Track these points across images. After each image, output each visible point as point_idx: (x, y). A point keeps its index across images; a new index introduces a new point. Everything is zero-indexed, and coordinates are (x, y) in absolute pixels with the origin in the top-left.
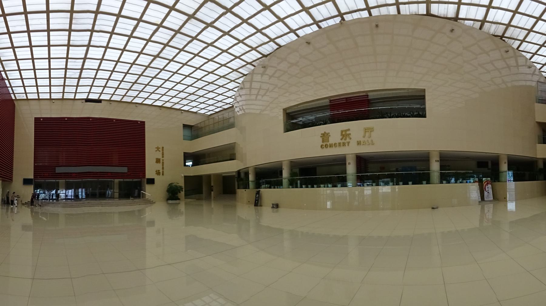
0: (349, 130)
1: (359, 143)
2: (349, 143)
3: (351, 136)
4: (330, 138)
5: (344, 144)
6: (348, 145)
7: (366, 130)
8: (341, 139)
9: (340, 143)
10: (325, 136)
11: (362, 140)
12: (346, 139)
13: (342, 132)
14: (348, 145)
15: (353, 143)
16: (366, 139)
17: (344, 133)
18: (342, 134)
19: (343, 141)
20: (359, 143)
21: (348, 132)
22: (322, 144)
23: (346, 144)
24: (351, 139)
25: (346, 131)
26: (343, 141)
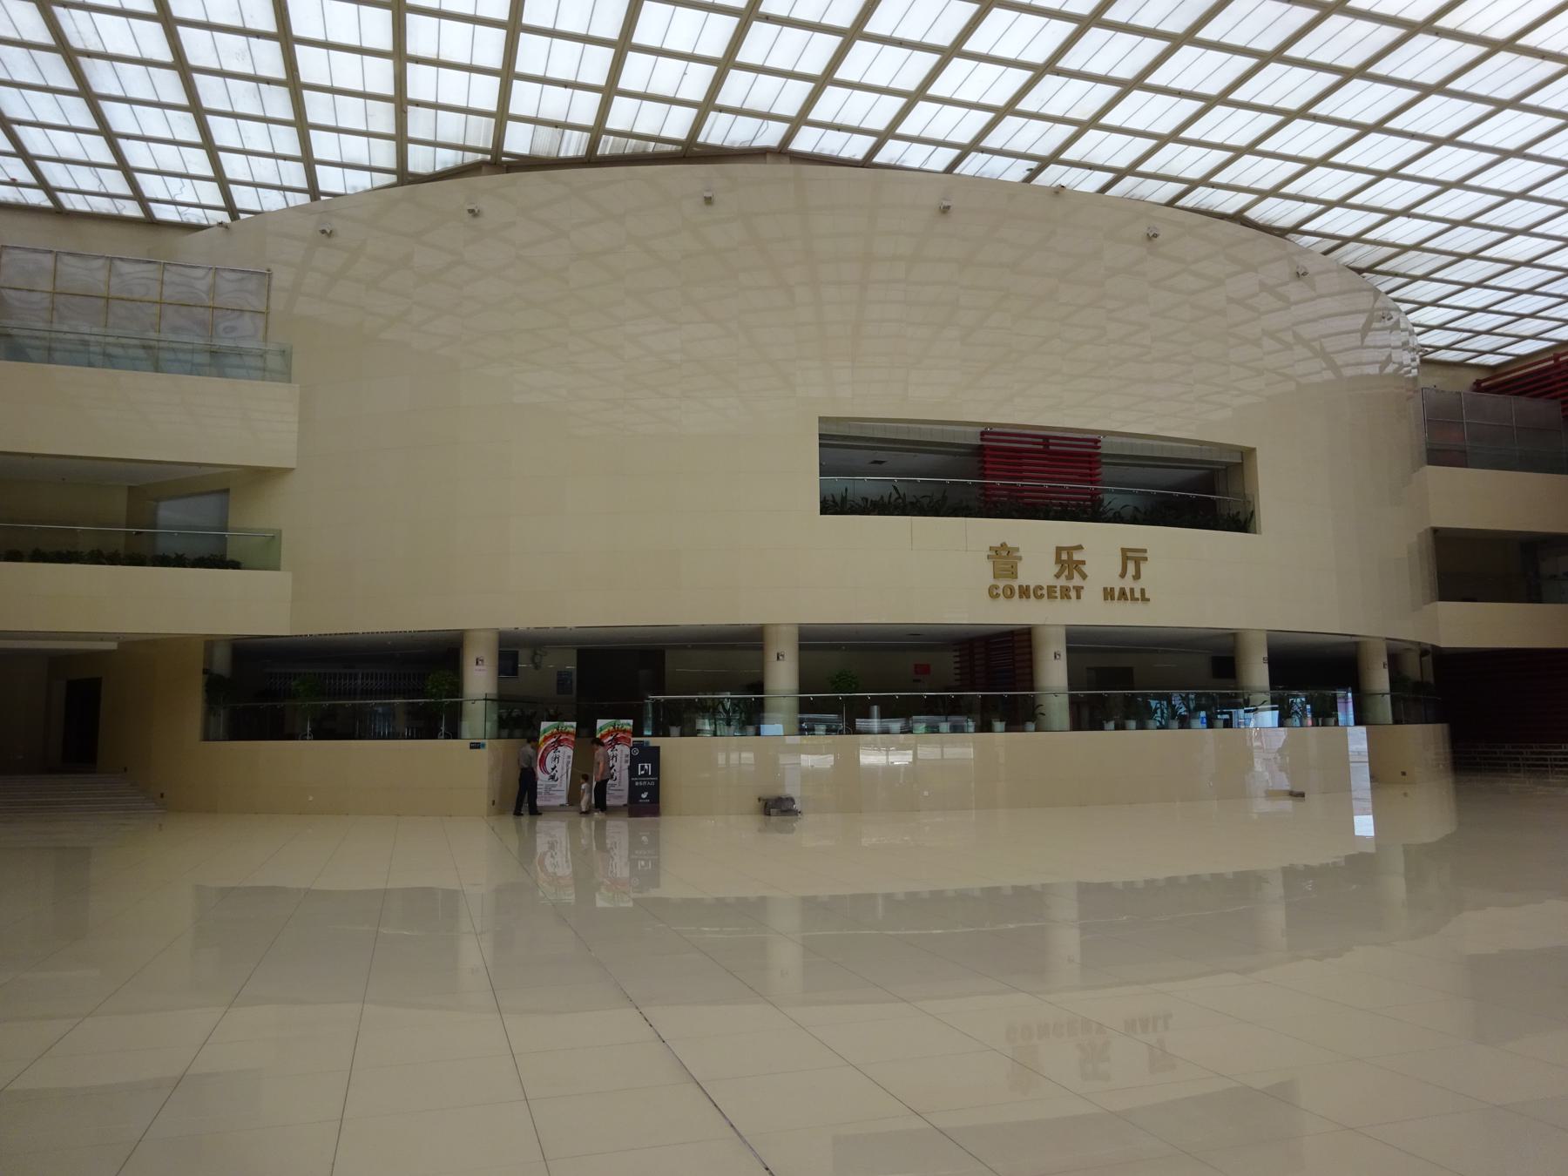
0: (1080, 548)
1: (1108, 594)
2: (1078, 590)
3: (1085, 569)
4: (1022, 569)
5: (1065, 593)
6: (1078, 597)
7: (1126, 555)
8: (1058, 576)
9: (1051, 589)
10: (1005, 560)
11: (1117, 584)
12: (1070, 577)
13: (1059, 550)
14: (1078, 597)
15: (1092, 591)
16: (1128, 583)
17: (1064, 556)
18: (1058, 560)
19: (1062, 582)
20: (1108, 594)
21: (1077, 556)
22: (992, 581)
23: (1073, 594)
24: (1084, 576)
25: (1070, 550)
26: (1062, 582)
